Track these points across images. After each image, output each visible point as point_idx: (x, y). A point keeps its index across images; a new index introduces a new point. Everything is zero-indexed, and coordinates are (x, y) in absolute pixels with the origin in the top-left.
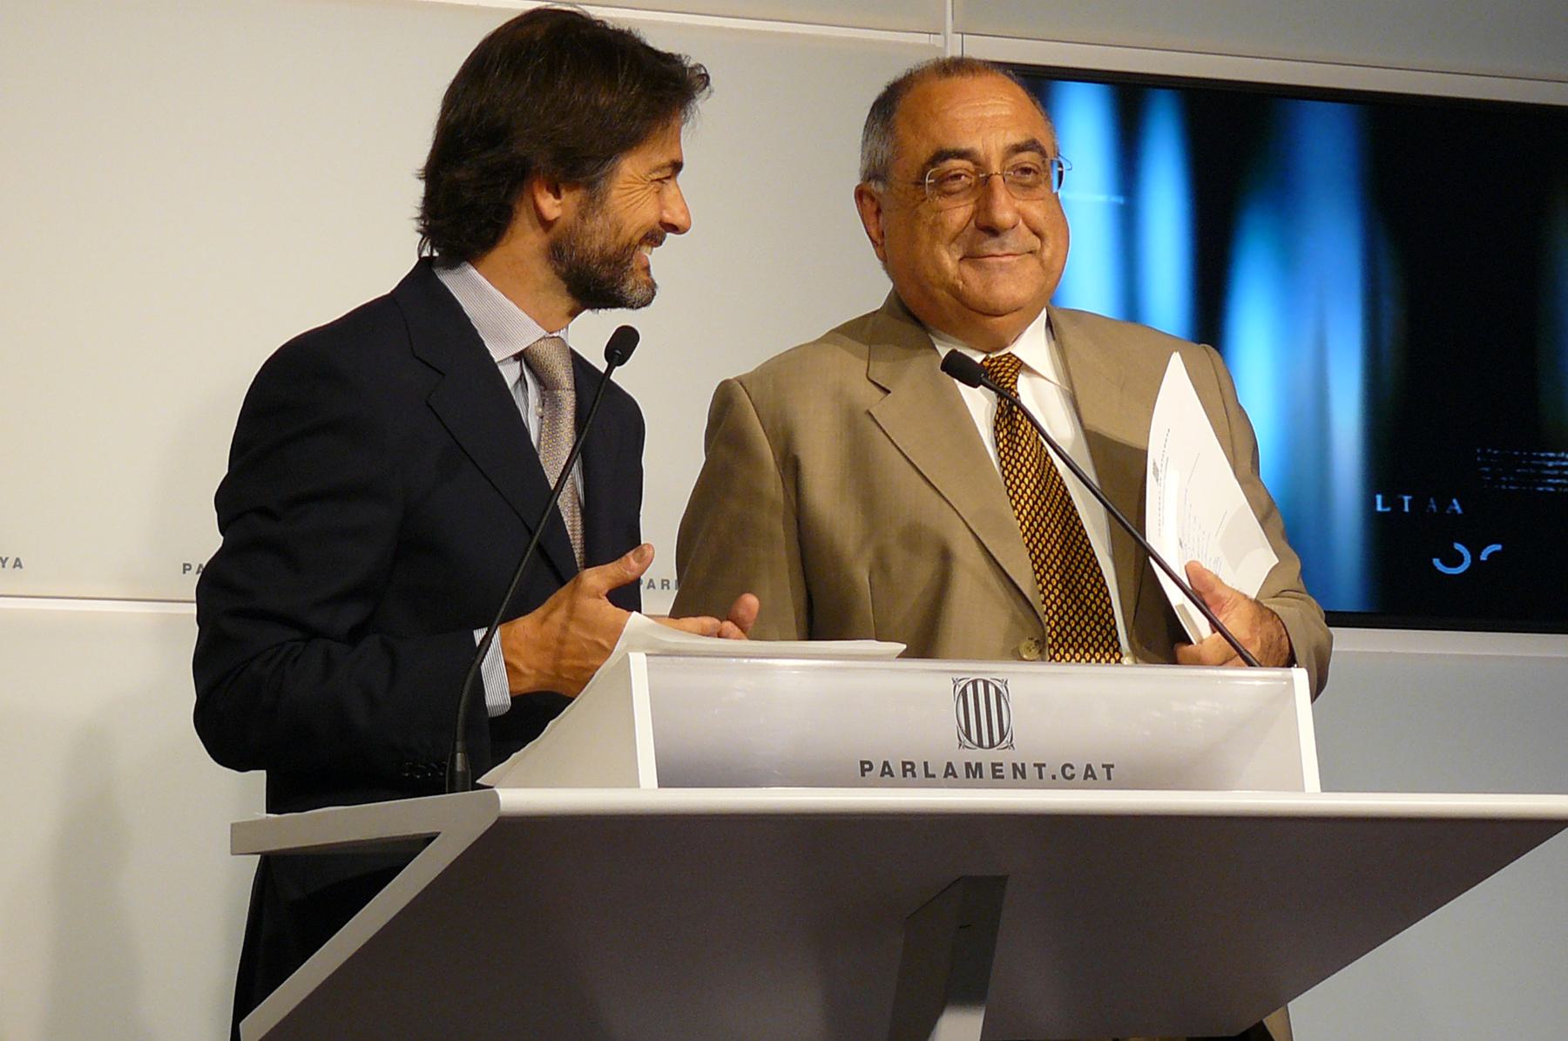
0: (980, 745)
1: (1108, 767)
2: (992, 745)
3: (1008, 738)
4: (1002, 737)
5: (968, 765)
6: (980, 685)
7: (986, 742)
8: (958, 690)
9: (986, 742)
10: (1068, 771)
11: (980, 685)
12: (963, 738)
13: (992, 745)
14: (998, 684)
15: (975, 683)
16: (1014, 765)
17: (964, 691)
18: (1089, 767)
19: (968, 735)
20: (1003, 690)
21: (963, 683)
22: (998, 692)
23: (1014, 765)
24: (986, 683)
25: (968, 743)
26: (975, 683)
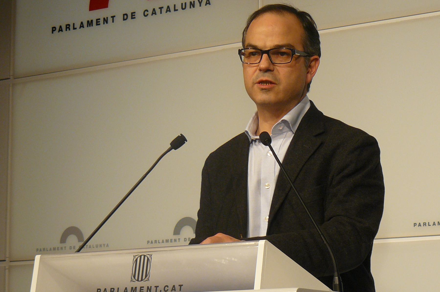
0: (138, 280)
1: (181, 286)
2: (142, 280)
3: (148, 277)
4: (146, 276)
5: (132, 288)
6: (143, 257)
7: (140, 279)
8: (135, 259)
9: (140, 279)
10: (166, 288)
11: (143, 257)
12: (133, 278)
13: (142, 280)
14: (149, 256)
15: (141, 256)
16: (148, 287)
17: (137, 260)
18: (174, 286)
19: (134, 277)
20: (150, 258)
21: (137, 257)
22: (148, 259)
23: (148, 287)
24: (145, 256)
25: (134, 280)
26: (141, 256)
